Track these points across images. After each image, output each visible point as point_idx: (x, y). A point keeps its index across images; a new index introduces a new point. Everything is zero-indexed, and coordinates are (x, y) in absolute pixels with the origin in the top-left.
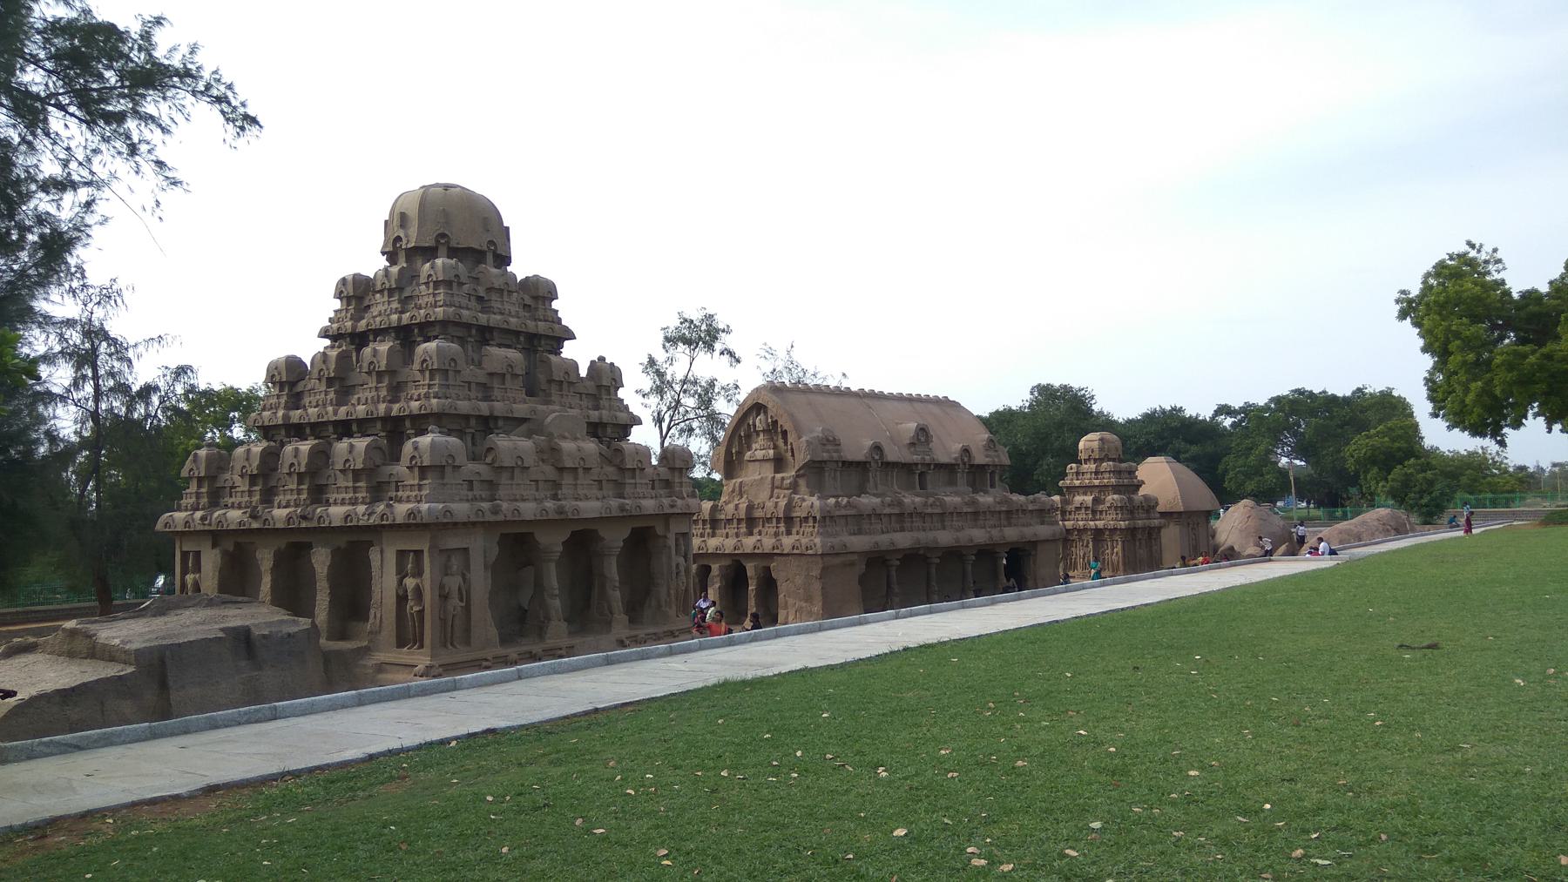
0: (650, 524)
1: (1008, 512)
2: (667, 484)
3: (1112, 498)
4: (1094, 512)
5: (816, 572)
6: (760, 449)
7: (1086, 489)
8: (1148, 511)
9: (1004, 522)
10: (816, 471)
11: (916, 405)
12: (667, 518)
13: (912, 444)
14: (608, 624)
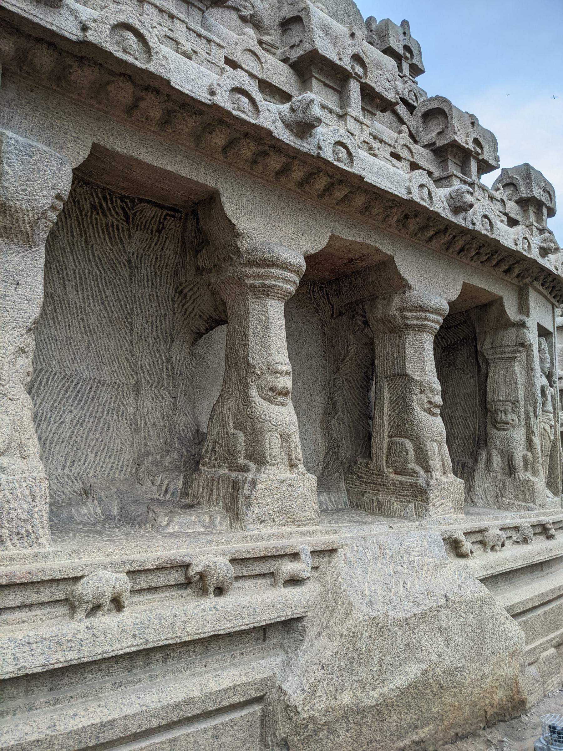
14: (420, 495)
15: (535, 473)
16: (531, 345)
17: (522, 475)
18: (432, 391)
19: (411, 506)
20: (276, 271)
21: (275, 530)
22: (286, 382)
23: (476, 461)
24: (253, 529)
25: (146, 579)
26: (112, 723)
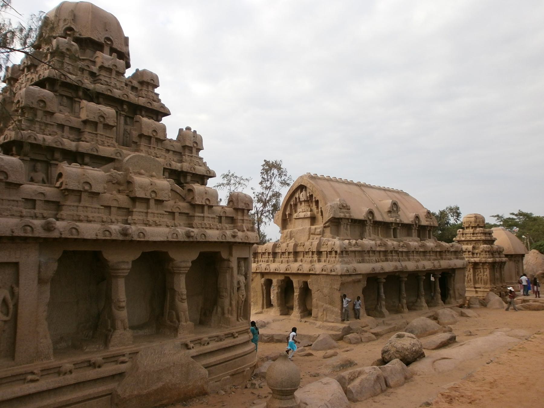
0: (217, 250)
1: (440, 252)
2: (232, 220)
3: (483, 246)
4: (473, 254)
5: (337, 286)
6: (303, 211)
7: (468, 242)
8: (499, 254)
9: (439, 257)
10: (336, 223)
11: (389, 193)
12: (230, 246)
13: (389, 212)
14: (175, 330)
15: (232, 314)
16: (232, 268)
17: (226, 316)
18: (182, 294)
19: (173, 333)
20: (120, 271)
21: (118, 348)
22: (124, 304)
23: (213, 310)
24: (111, 349)
25: (78, 366)
26: (70, 400)
